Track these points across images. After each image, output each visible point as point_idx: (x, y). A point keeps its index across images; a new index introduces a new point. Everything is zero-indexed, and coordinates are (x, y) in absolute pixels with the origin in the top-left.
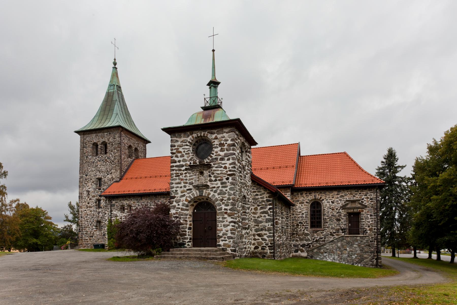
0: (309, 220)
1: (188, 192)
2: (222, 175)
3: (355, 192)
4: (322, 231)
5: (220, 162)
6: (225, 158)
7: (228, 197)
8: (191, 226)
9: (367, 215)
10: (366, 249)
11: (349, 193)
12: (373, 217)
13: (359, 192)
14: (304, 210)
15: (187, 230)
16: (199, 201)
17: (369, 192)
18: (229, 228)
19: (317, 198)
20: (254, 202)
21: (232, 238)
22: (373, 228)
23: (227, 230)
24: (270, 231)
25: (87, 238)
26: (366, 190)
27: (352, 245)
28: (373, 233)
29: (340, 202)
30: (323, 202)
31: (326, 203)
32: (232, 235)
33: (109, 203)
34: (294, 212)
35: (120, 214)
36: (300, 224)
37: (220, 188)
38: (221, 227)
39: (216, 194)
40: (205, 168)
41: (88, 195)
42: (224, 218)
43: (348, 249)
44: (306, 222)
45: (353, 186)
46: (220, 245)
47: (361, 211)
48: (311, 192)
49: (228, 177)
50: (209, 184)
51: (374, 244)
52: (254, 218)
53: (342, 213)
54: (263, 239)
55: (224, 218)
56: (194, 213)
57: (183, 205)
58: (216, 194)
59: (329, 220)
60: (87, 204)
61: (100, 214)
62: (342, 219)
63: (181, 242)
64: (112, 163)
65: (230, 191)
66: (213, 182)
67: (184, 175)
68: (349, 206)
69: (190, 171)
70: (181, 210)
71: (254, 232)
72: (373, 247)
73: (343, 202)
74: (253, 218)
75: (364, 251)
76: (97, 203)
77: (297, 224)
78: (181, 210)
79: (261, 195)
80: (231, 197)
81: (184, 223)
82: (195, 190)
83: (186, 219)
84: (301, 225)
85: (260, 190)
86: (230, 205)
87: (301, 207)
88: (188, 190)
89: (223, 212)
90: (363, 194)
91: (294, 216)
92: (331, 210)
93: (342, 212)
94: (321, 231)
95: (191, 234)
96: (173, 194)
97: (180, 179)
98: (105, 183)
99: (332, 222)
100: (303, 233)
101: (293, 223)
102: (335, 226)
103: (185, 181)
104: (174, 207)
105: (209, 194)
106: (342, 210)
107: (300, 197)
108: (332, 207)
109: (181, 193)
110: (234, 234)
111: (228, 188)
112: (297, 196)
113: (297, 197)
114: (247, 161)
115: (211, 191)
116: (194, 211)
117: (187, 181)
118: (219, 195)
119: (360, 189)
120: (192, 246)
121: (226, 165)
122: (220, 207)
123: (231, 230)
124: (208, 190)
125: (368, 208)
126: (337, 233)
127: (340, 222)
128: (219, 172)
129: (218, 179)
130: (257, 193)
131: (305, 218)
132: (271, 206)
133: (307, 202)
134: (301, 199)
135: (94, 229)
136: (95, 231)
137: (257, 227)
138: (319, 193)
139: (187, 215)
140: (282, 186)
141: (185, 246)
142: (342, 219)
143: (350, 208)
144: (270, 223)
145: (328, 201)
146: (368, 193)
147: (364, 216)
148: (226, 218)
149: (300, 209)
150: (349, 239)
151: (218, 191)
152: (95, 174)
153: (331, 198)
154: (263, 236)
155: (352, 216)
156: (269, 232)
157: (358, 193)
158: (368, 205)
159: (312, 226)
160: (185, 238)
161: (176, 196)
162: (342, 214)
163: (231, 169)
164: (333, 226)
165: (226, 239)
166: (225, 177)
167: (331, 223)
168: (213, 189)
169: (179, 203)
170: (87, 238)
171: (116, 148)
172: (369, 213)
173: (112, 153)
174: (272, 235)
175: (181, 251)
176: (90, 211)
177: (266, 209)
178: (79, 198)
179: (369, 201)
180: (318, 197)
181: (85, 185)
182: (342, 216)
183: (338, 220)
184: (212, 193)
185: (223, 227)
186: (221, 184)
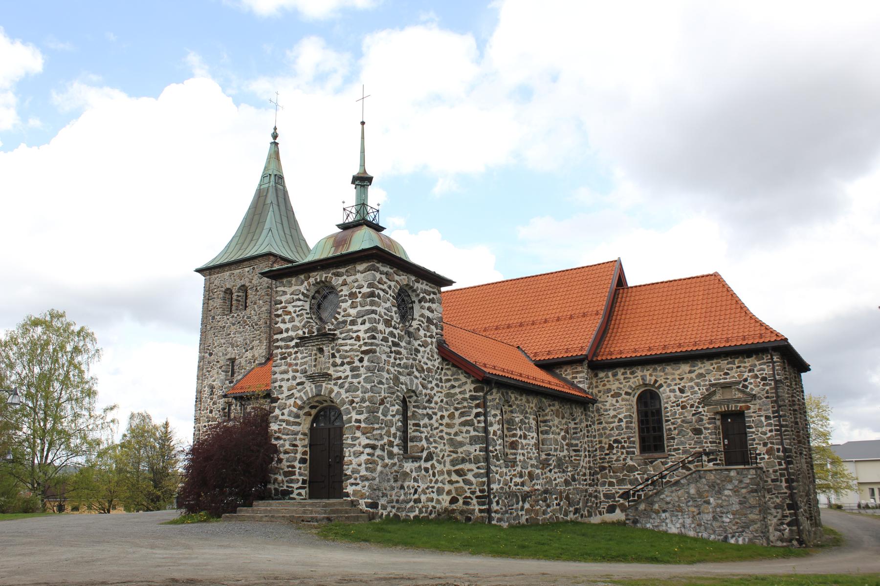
0: (637, 435)
1: (299, 387)
2: (352, 353)
3: (728, 364)
4: (663, 458)
5: (350, 327)
6: (358, 319)
7: (361, 395)
8: (307, 455)
9: (758, 416)
10: (752, 499)
11: (714, 368)
12: (772, 421)
13: (736, 363)
14: (622, 412)
15: (297, 464)
16: (321, 406)
17: (757, 363)
18: (364, 457)
19: (647, 382)
20: (447, 403)
21: (367, 479)
22: (776, 447)
23: (359, 463)
24: (479, 463)
26: (750, 359)
27: (720, 492)
28: (776, 461)
29: (696, 389)
30: (661, 390)
31: (668, 393)
32: (368, 474)
33: (241, 409)
34: (602, 418)
36: (615, 445)
37: (349, 379)
38: (350, 456)
39: (342, 391)
40: (323, 341)
41: (211, 394)
42: (354, 439)
43: (712, 500)
44: (629, 438)
45: (719, 350)
46: (347, 495)
48: (634, 369)
51: (781, 486)
52: (449, 437)
53: (703, 415)
55: (354, 439)
56: (312, 429)
57: (289, 415)
58: (342, 391)
59: (676, 432)
62: (706, 429)
63: (285, 488)
64: (255, 327)
65: (365, 384)
67: (294, 356)
69: (302, 348)
70: (286, 425)
71: (449, 467)
72: (778, 493)
73: (704, 388)
74: (446, 437)
75: (747, 505)
76: (226, 410)
77: (610, 445)
78: (286, 425)
79: (459, 386)
80: (367, 395)
82: (309, 384)
83: (294, 442)
84: (617, 447)
85: (458, 377)
87: (615, 404)
88: (298, 384)
89: (354, 425)
90: (745, 367)
91: (602, 426)
92: (679, 408)
93: (704, 411)
94: (663, 460)
95: (306, 472)
96: (276, 393)
99: (683, 436)
100: (624, 465)
101: (600, 442)
102: (692, 446)
103: (294, 367)
104: (277, 417)
105: (331, 391)
106: (702, 407)
107: (611, 383)
108: (682, 402)
109: (288, 390)
110: (372, 470)
111: (361, 379)
112: (606, 380)
113: (606, 382)
115: (335, 384)
116: (312, 425)
119: (737, 358)
120: (307, 496)
122: (349, 416)
123: (366, 464)
124: (330, 384)
125: (758, 401)
126: (696, 464)
127: (702, 436)
128: (347, 348)
129: (345, 361)
130: (453, 383)
131: (625, 430)
132: (479, 410)
133: (627, 393)
134: (614, 386)
137: (454, 455)
138: (651, 370)
139: (296, 434)
141: (291, 496)
142: (706, 429)
143: (719, 403)
144: (478, 447)
145: (671, 388)
146: (755, 366)
147: (751, 419)
148: (359, 438)
149: (614, 410)
150: (713, 477)
151: (347, 385)
152: (226, 350)
153: (678, 381)
154: (466, 475)
155: (729, 420)
156: (477, 466)
157: (734, 366)
158: (759, 393)
159: (644, 449)
160: (292, 481)
161: (280, 396)
162: (704, 417)
163: (366, 341)
164: (687, 446)
165: (358, 481)
166: (357, 356)
167: (682, 439)
168: (338, 381)
169: (283, 411)
171: (263, 296)
172: (762, 413)
173: (255, 306)
174: (482, 471)
175: (271, 505)
177: (470, 416)
178: (196, 402)
179: (760, 383)
180: (650, 380)
181: (207, 373)
182: (704, 422)
183: (698, 432)
184: (336, 389)
185: (352, 458)
186: (351, 371)
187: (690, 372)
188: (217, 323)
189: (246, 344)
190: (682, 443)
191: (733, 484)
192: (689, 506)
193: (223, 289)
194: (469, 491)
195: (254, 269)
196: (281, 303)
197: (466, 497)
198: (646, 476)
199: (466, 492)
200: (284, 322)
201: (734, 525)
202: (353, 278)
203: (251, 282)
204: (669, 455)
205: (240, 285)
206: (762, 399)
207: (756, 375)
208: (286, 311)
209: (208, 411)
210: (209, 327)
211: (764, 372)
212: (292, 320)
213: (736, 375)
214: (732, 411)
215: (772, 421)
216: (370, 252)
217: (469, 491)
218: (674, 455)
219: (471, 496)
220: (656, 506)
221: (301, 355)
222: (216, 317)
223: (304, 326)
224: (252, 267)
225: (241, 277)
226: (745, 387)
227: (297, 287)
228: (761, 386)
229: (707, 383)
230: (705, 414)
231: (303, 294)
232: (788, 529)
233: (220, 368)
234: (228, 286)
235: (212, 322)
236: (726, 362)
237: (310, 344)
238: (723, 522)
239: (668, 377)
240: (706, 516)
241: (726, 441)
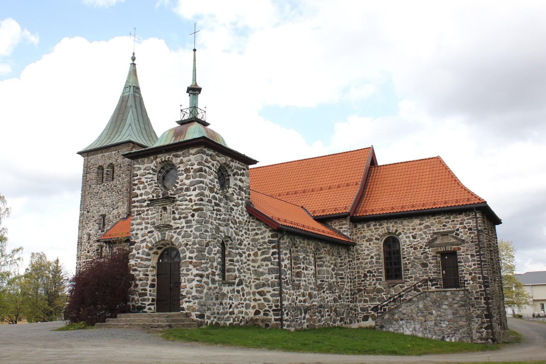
0: (383, 267)
1: (150, 235)
2: (186, 211)
3: (446, 219)
4: (401, 283)
5: (185, 193)
6: (191, 187)
7: (193, 240)
8: (155, 282)
9: (466, 255)
10: (461, 311)
11: (436, 222)
12: (475, 258)
13: (451, 218)
14: (374, 252)
15: (148, 288)
16: (165, 247)
17: (466, 218)
18: (195, 283)
19: (391, 231)
20: (253, 245)
21: (197, 298)
22: (478, 275)
23: (191, 287)
24: (274, 287)
26: (461, 216)
27: (439, 306)
28: (478, 285)
29: (424, 236)
30: (400, 236)
31: (405, 239)
32: (198, 294)
33: (110, 250)
34: (360, 256)
36: (368, 274)
37: (185, 229)
38: (185, 282)
39: (180, 237)
40: (167, 202)
41: (88, 240)
42: (188, 270)
43: (434, 312)
45: (440, 209)
46: (183, 309)
47: (456, 249)
49: (193, 213)
50: (172, 223)
51: (481, 302)
52: (254, 269)
53: (429, 254)
54: (266, 300)
55: (188, 270)
56: (158, 263)
57: (143, 254)
58: (180, 237)
59: (410, 265)
63: (140, 304)
64: (119, 193)
65: (195, 232)
66: (177, 221)
67: (146, 213)
68: (438, 242)
69: (152, 207)
70: (141, 261)
71: (254, 289)
72: (479, 307)
73: (429, 235)
74: (252, 269)
75: (458, 315)
76: (99, 251)
77: (365, 274)
78: (141, 261)
79: (261, 234)
80: (197, 240)
81: (144, 278)
82: (157, 232)
83: (146, 273)
84: (370, 276)
85: (260, 227)
86: (195, 251)
87: (369, 246)
88: (149, 232)
89: (188, 261)
90: (457, 221)
91: (360, 261)
93: (429, 251)
94: (401, 285)
95: (154, 294)
96: (133, 238)
97: (141, 218)
98: (110, 221)
99: (415, 268)
100: (375, 288)
102: (421, 275)
103: (146, 221)
104: (134, 255)
105: (172, 237)
106: (428, 249)
107: (366, 232)
108: (414, 245)
111: (193, 229)
112: (362, 229)
113: (362, 231)
114: (236, 187)
115: (175, 232)
116: (159, 261)
117: (149, 221)
118: (183, 239)
119: (452, 215)
120: (155, 310)
122: (184, 254)
123: (196, 287)
124: (172, 232)
125: (466, 244)
126: (423, 287)
127: (428, 268)
128: (183, 207)
129: (182, 216)
130: (257, 231)
131: (375, 264)
132: (275, 250)
133: (377, 239)
137: (258, 282)
138: (393, 223)
139: (148, 267)
140: (333, 216)
141: (144, 310)
143: (440, 246)
144: (274, 276)
145: (407, 235)
147: (461, 257)
148: (191, 270)
149: (368, 250)
150: (435, 296)
151: (183, 233)
153: (411, 231)
154: (265, 295)
155: (446, 257)
156: (273, 289)
157: (450, 220)
158: (467, 239)
159: (388, 277)
160: (144, 300)
161: (136, 241)
162: (429, 255)
164: (418, 275)
165: (191, 299)
166: (190, 213)
167: (414, 270)
168: (177, 230)
169: (139, 251)
171: (125, 171)
172: (469, 252)
173: (120, 178)
174: (277, 292)
175: (129, 317)
177: (268, 254)
178: (78, 245)
180: (393, 230)
181: (86, 225)
182: (429, 258)
183: (425, 265)
184: (175, 236)
185: (187, 283)
186: (186, 223)
187: (420, 224)
188: (92, 190)
189: (113, 204)
190: (414, 273)
191: (449, 301)
192: (418, 316)
193: (97, 166)
194: (268, 306)
195: (118, 152)
196: (137, 175)
197: (265, 311)
198: (389, 296)
199: (265, 307)
200: (139, 189)
201: (449, 329)
202: (187, 158)
203: (116, 161)
204: (405, 281)
205: (109, 163)
206: (468, 243)
207: (465, 226)
208: (140, 181)
209: (87, 251)
210: (87, 193)
211: (471, 225)
212: (145, 188)
213: (451, 226)
214: (448, 251)
215: (475, 258)
216: (199, 141)
217: (268, 306)
218: (408, 281)
219: (269, 309)
220: (396, 316)
221: (151, 212)
222: (92, 186)
223: (153, 192)
224: (117, 151)
228: (468, 234)
229: (432, 232)
230: (430, 253)
231: (152, 169)
232: (485, 331)
233: (95, 221)
234: (100, 164)
235: (89, 189)
236: (444, 217)
237: (157, 205)
238: (442, 327)
239: (405, 228)
240: (430, 323)
241: (444, 271)
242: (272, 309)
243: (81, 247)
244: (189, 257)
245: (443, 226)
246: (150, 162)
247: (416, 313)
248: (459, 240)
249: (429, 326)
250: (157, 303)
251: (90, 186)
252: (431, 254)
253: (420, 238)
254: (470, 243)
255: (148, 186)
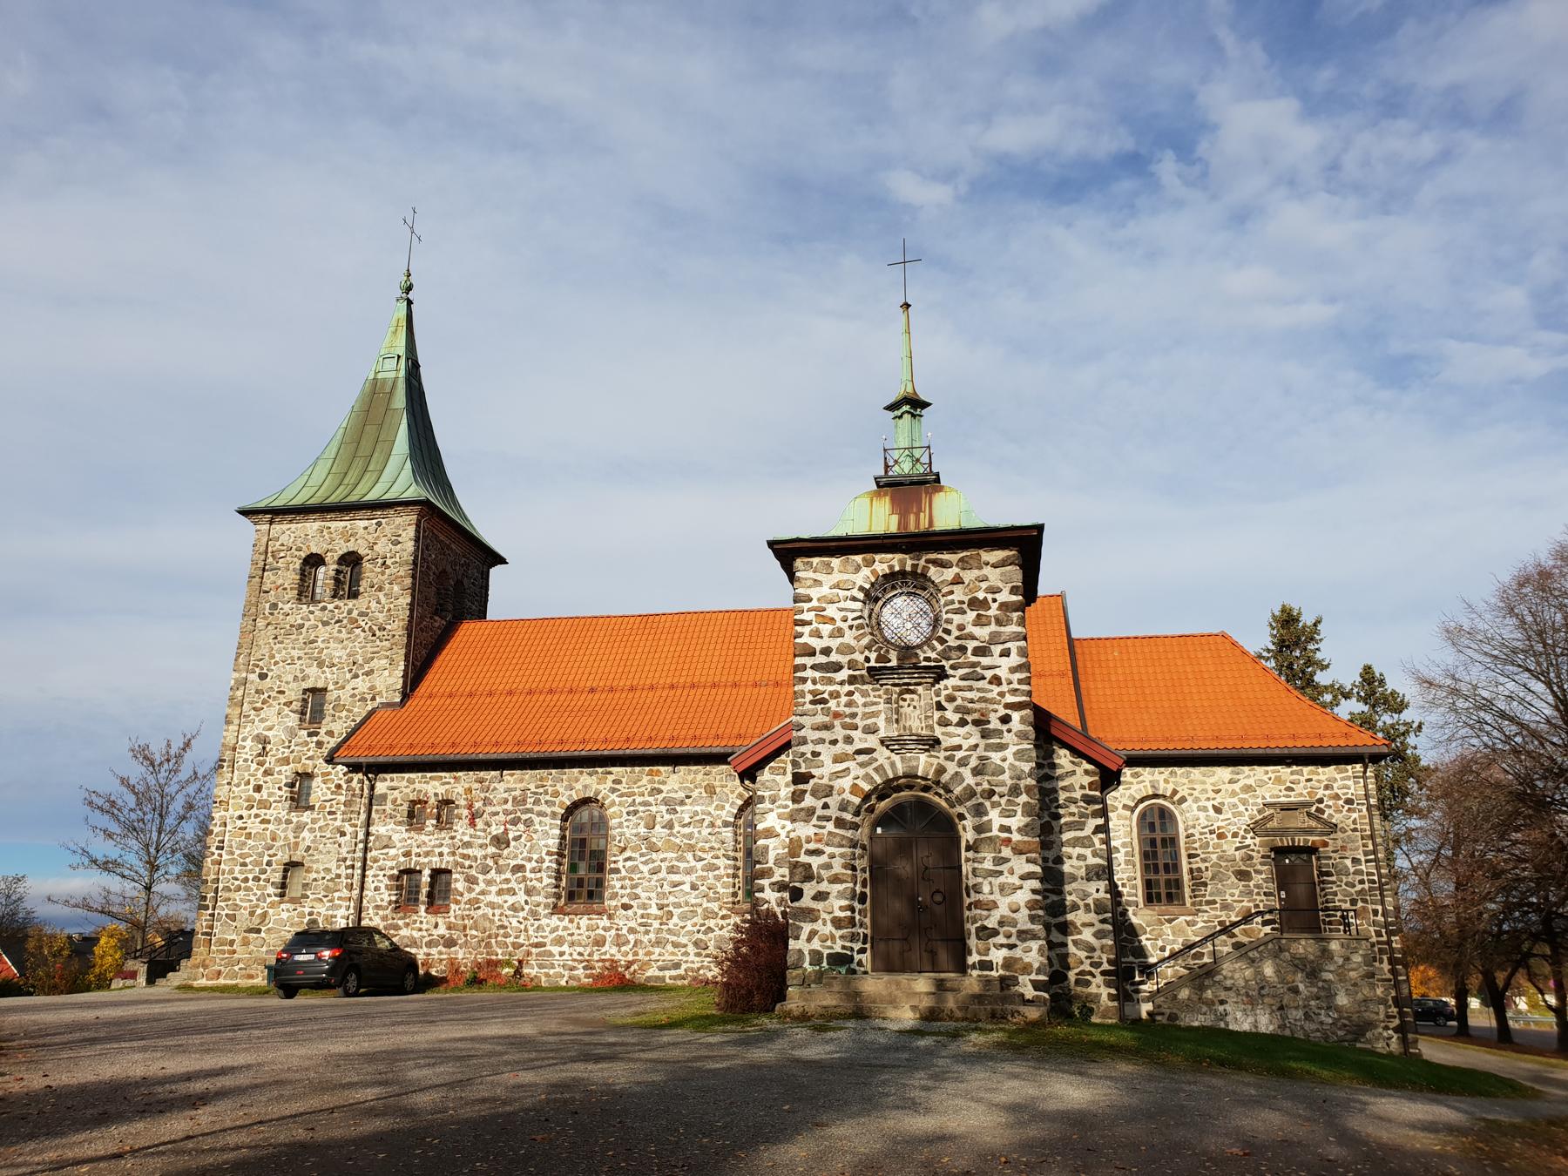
1: (862, 758)
6: (992, 647)
7: (1009, 782)
25: (234, 937)
28: (1372, 929)
29: (1242, 808)
31: (1196, 812)
35: (406, 835)
39: (966, 772)
47: (1318, 845)
50: (938, 732)
53: (1253, 850)
59: (1209, 874)
60: (251, 792)
61: (305, 834)
62: (1257, 872)
64: (378, 633)
67: (844, 699)
68: (1274, 824)
69: (865, 687)
86: (1019, 812)
88: (859, 752)
89: (998, 837)
92: (1214, 836)
96: (803, 765)
97: (827, 712)
102: (1236, 898)
103: (848, 720)
108: (1219, 828)
117: (857, 720)
118: (979, 777)
121: (997, 672)
127: (1252, 883)
129: (969, 718)
135: (269, 895)
136: (272, 905)
142: (1257, 872)
143: (1282, 832)
145: (1200, 804)
147: (1330, 862)
148: (1007, 860)
151: (973, 762)
153: (1212, 795)
156: (1101, 917)
161: (814, 772)
162: (1254, 854)
170: (230, 938)
173: (381, 595)
176: (262, 822)
181: (253, 712)
182: (1254, 861)
186: (983, 737)
187: (1231, 782)
188: (281, 617)
189: (354, 663)
190: (1220, 893)
191: (1336, 963)
192: (1263, 996)
193: (304, 555)
194: (1089, 961)
195: (379, 524)
196: (810, 600)
197: (1082, 973)
198: (1160, 943)
199: (1082, 963)
200: (817, 634)
201: (1340, 1029)
202: (975, 573)
203: (371, 548)
204: (1199, 910)
205: (346, 551)
206: (1346, 831)
207: (1337, 794)
208: (823, 616)
209: (251, 787)
210: (261, 623)
211: (1350, 792)
212: (839, 633)
213: (1305, 792)
214: (1299, 846)
215: (1363, 867)
216: (1025, 534)
217: (1089, 961)
218: (1207, 911)
219: (1093, 970)
220: (1209, 994)
221: (864, 700)
222: (280, 605)
223: (869, 647)
224: (374, 521)
225: (348, 536)
226: (1323, 812)
227: (846, 577)
228: (1344, 813)
229: (1260, 801)
230: (1256, 849)
231: (861, 589)
232: (1396, 1036)
233: (288, 704)
234: (314, 550)
235: (272, 614)
236: (1289, 770)
237: (891, 681)
238: (1322, 1023)
239: (1195, 787)
240: (1294, 1013)
241: (1283, 893)
242: (1099, 970)
243: (233, 772)
244: (1001, 826)
245: (1286, 789)
246: (851, 569)
247: (1257, 987)
248: (1326, 823)
249: (1292, 1021)
250: (872, 947)
251: (274, 606)
252: (1258, 852)
253: (1233, 813)
254: (1350, 832)
255: (847, 632)
